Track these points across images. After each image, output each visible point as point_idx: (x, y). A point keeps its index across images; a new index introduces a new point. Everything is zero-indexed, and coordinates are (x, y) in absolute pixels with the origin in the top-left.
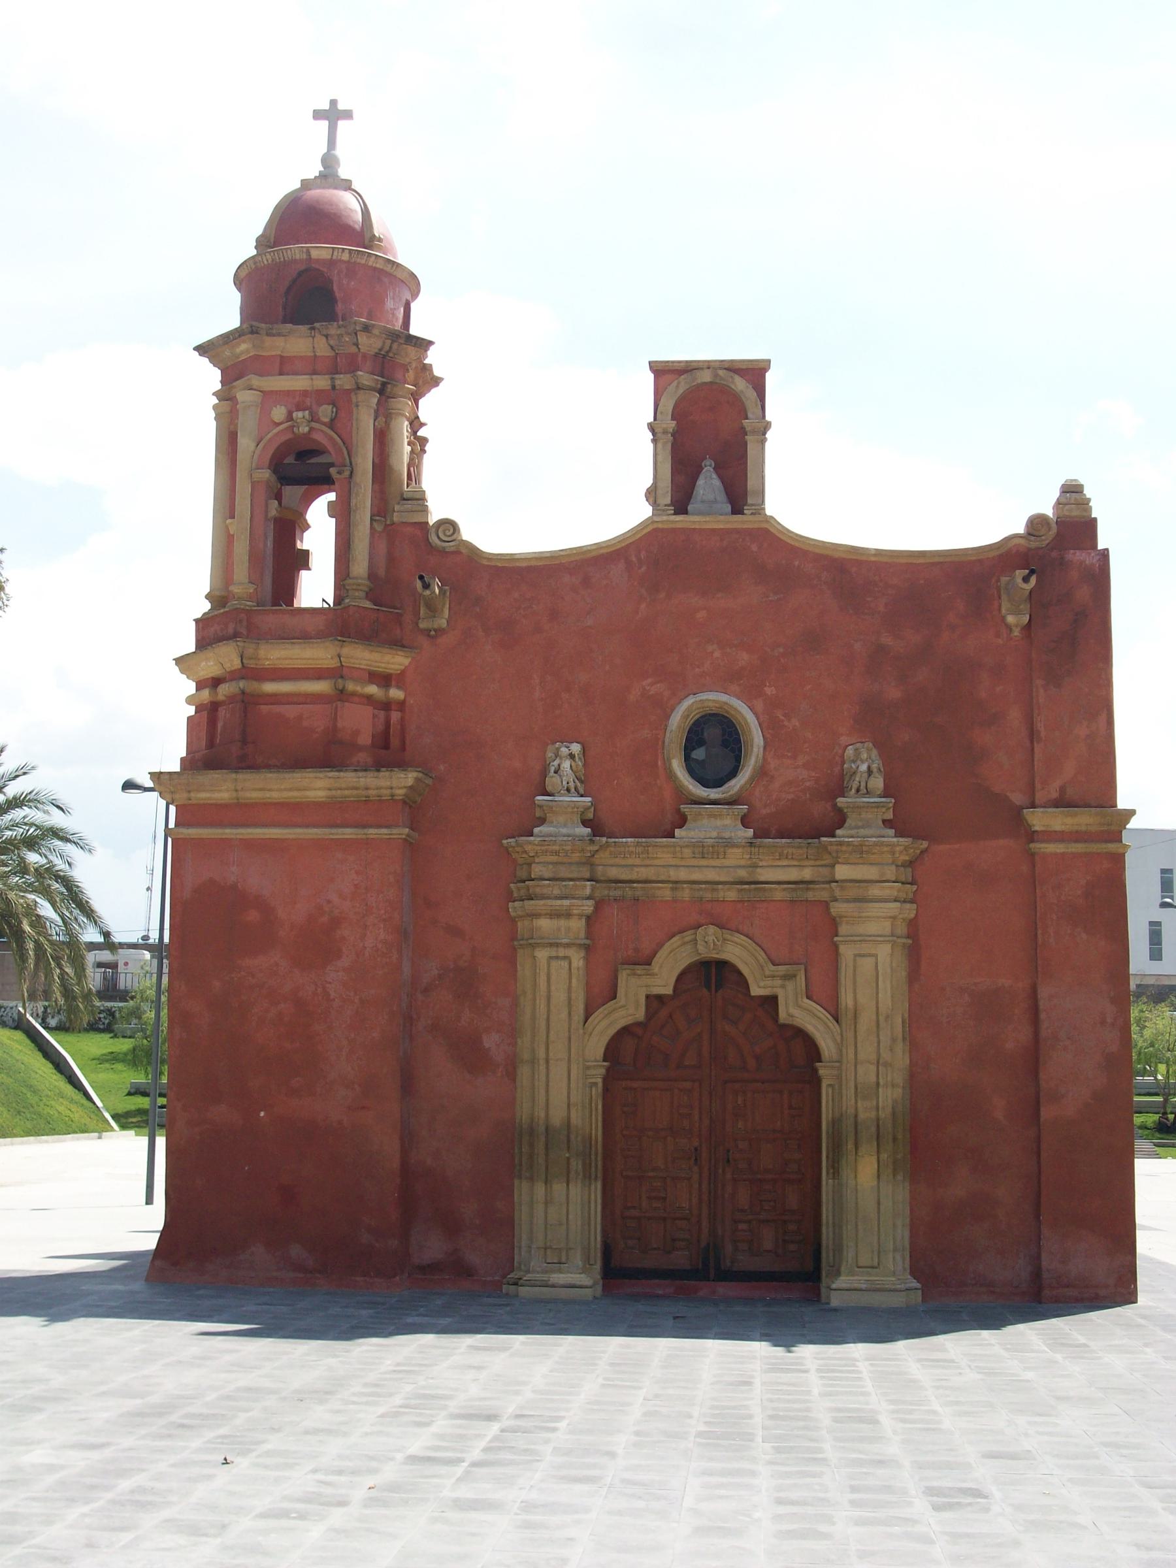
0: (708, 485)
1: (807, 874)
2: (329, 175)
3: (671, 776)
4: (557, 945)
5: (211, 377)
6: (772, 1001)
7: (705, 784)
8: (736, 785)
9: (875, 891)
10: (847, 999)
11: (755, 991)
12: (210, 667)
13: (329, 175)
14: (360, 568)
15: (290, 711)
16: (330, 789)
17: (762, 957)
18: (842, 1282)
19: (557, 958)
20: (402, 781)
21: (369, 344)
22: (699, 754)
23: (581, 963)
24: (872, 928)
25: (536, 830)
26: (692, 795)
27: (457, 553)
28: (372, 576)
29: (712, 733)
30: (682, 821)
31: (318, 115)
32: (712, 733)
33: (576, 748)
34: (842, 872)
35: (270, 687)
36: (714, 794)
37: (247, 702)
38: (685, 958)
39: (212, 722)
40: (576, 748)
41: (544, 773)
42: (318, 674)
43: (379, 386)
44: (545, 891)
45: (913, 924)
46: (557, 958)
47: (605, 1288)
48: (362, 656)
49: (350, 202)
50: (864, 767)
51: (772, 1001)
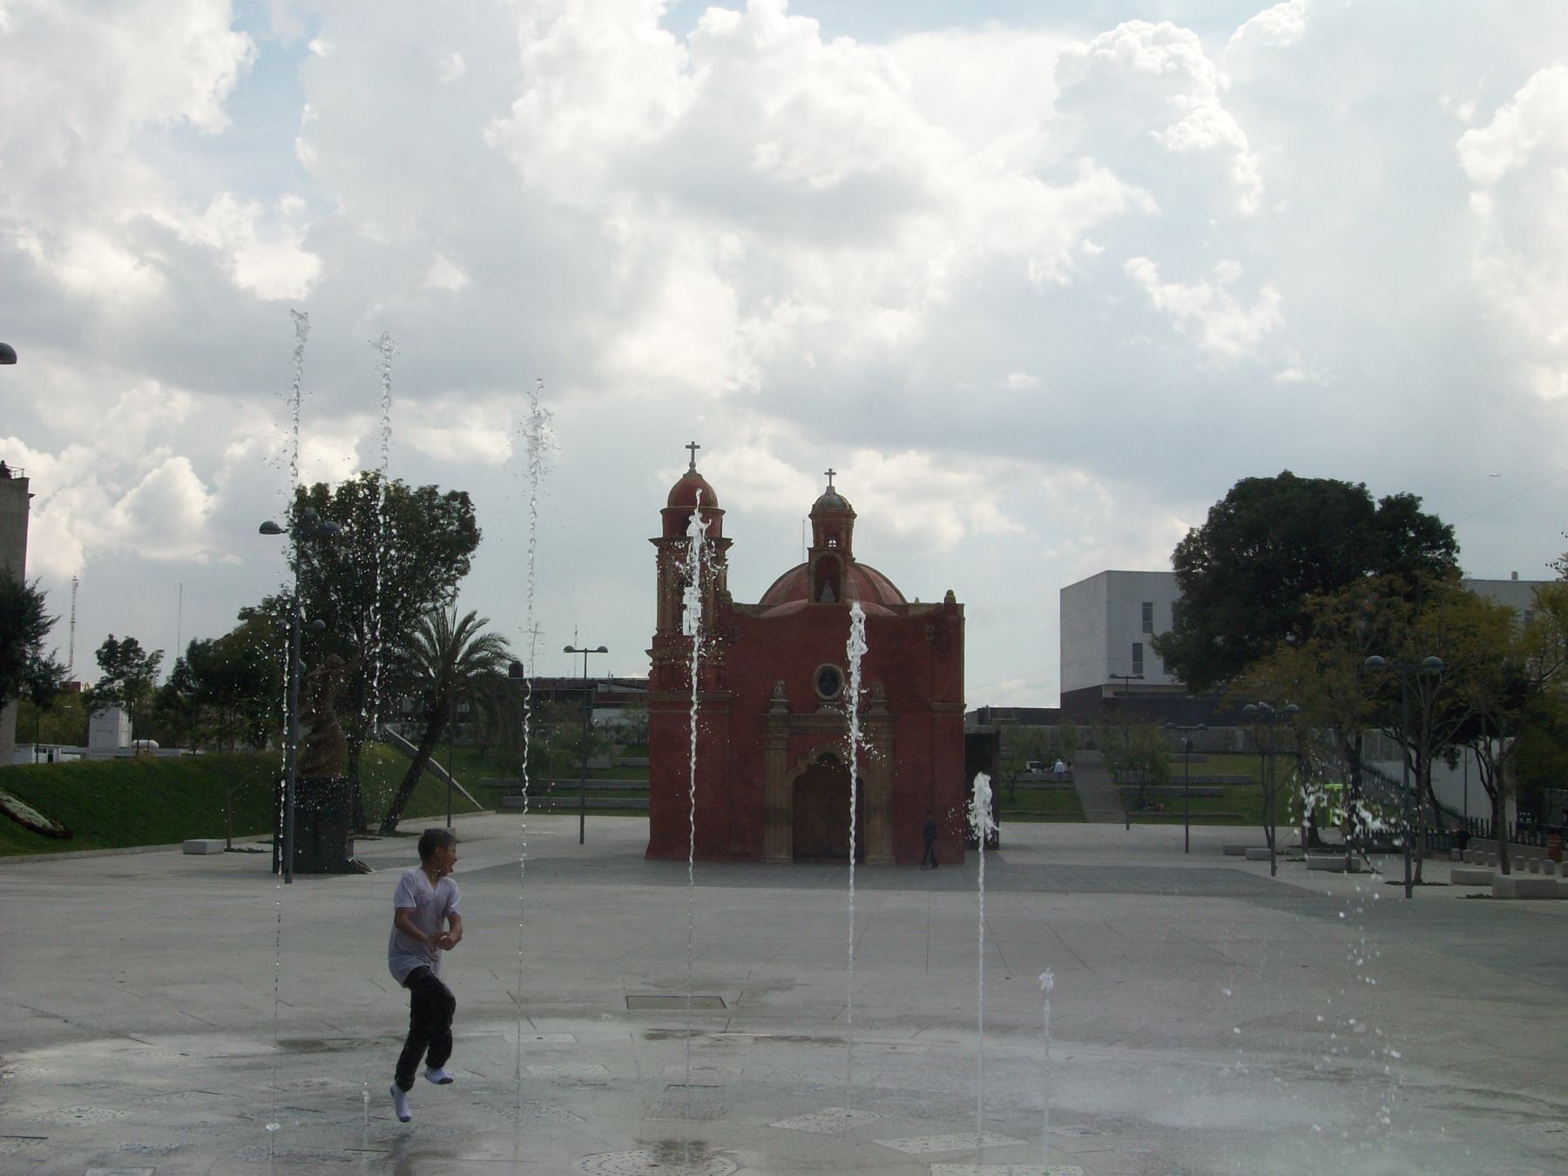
0: (827, 591)
3: (815, 693)
5: (655, 550)
7: (827, 694)
18: (870, 857)
25: (771, 711)
30: (818, 707)
36: (828, 698)
40: (783, 682)
41: (773, 690)
50: (878, 689)
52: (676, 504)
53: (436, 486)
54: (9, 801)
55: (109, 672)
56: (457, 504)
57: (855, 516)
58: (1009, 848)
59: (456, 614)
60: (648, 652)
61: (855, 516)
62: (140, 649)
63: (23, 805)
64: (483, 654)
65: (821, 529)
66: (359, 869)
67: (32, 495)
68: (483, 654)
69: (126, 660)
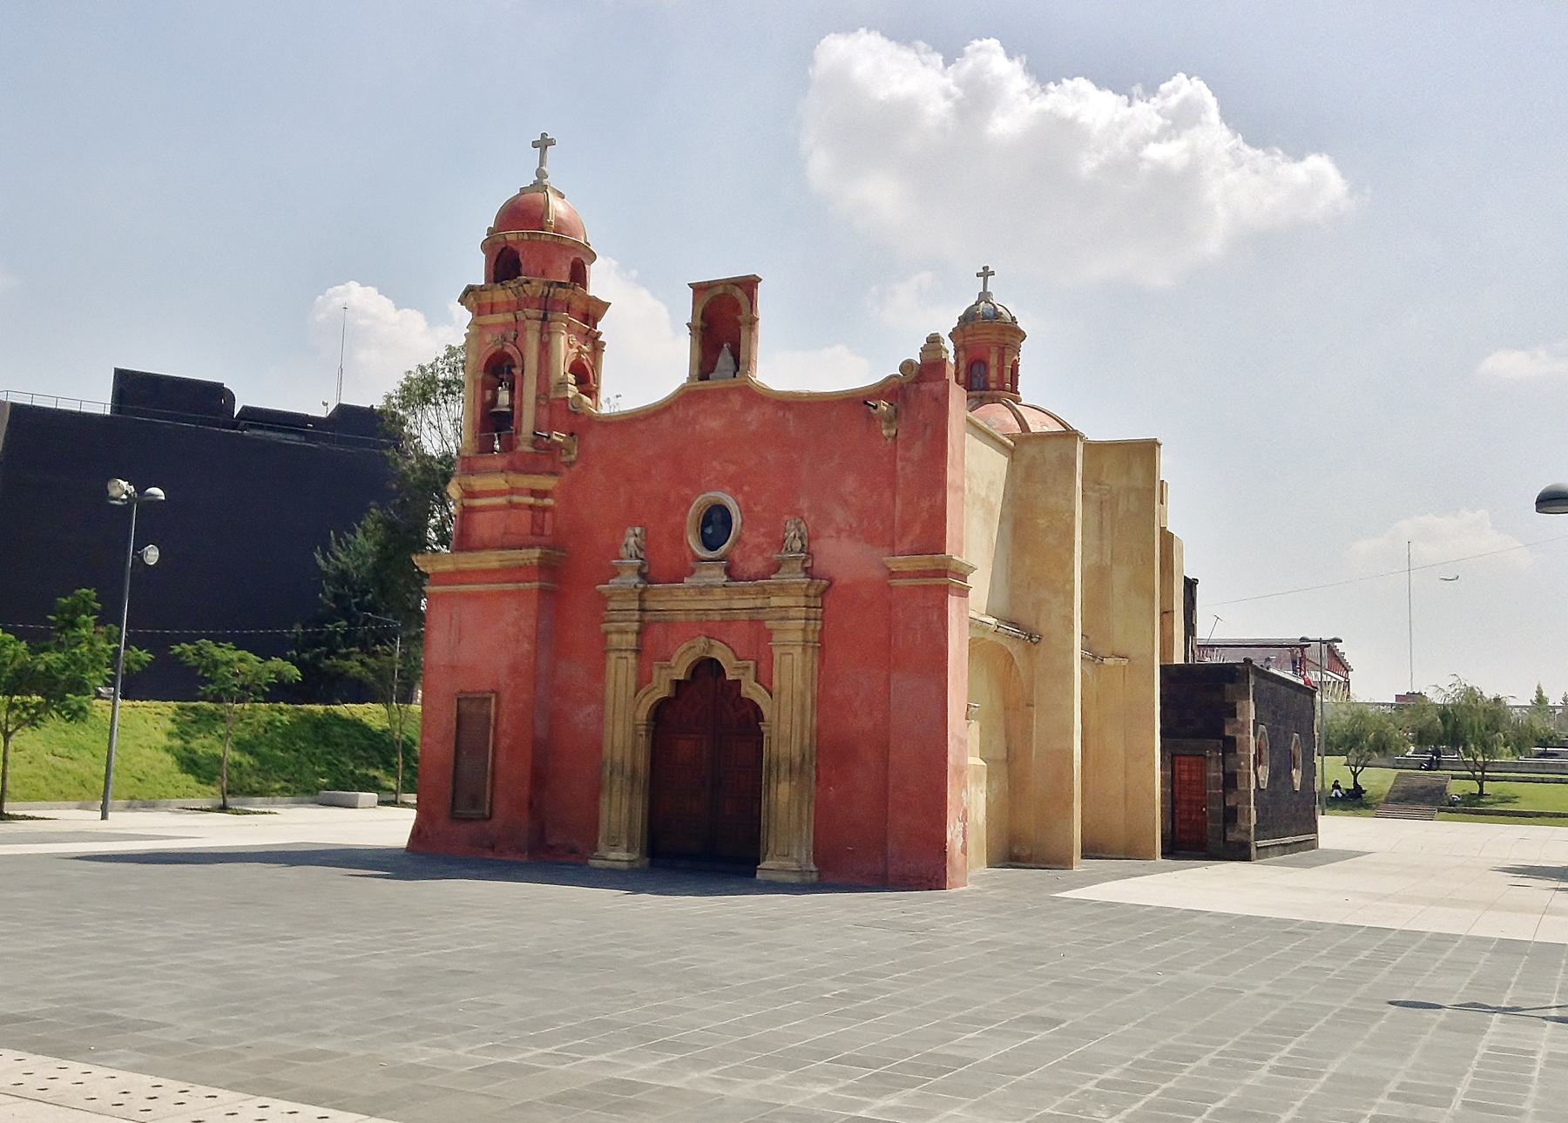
1: (759, 603)
2: (540, 186)
4: (621, 650)
6: (738, 682)
7: (712, 548)
8: (724, 548)
9: (792, 613)
10: (776, 683)
11: (729, 677)
16: (500, 561)
17: (731, 654)
19: (621, 658)
22: (709, 531)
23: (634, 661)
24: (791, 637)
26: (698, 555)
27: (583, 414)
29: (717, 516)
31: (535, 144)
32: (717, 516)
33: (638, 530)
38: (689, 659)
40: (638, 530)
43: (541, 316)
44: (615, 617)
46: (621, 658)
47: (652, 864)
51: (738, 682)
65: (961, 354)
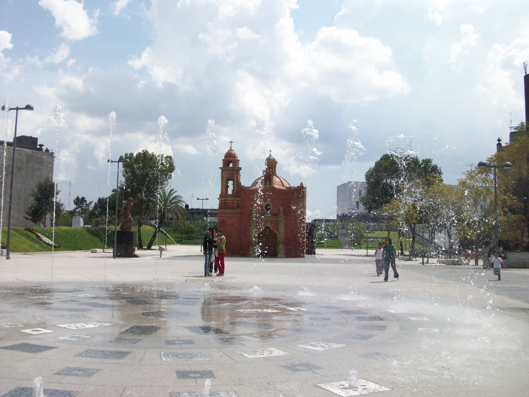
0: (268, 182)
1: (276, 219)
2: (231, 149)
5: (220, 171)
6: (273, 231)
10: (279, 231)
12: (221, 199)
13: (231, 149)
14: (235, 190)
15: (228, 204)
20: (239, 210)
21: (236, 169)
28: (236, 191)
31: (230, 142)
34: (279, 219)
35: (227, 202)
37: (225, 203)
39: (221, 204)
42: (231, 200)
45: (286, 224)
48: (236, 199)
49: (233, 152)
51: (273, 231)
52: (226, 158)
53: (163, 154)
54: (43, 237)
55: (77, 206)
56: (169, 159)
57: (277, 163)
58: (317, 254)
59: (167, 190)
60: (218, 199)
61: (277, 163)
62: (86, 200)
63: (47, 239)
64: (175, 200)
66: (136, 256)
67: (55, 157)
68: (175, 200)
69: (82, 203)
